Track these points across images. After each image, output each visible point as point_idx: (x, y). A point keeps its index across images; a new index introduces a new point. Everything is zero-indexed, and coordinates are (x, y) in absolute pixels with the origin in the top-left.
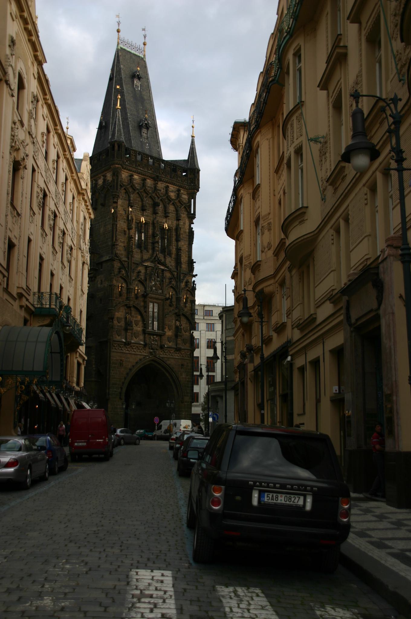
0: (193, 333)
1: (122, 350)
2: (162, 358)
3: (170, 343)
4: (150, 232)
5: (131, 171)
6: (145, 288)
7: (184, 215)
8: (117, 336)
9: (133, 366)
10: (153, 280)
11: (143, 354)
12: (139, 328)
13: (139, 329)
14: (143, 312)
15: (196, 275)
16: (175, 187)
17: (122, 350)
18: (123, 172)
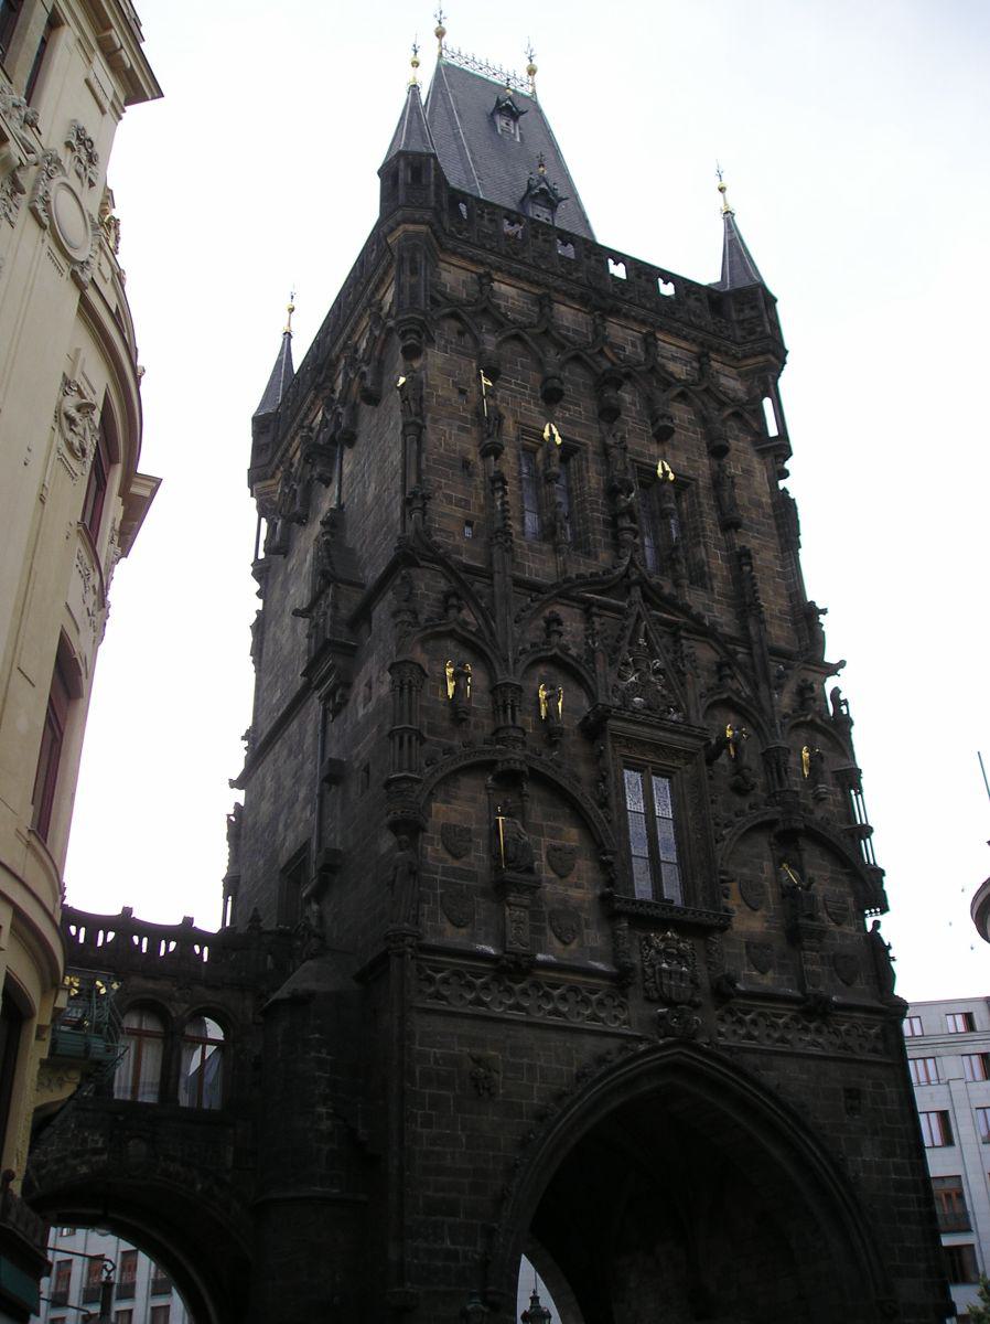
0: (877, 924)
1: (483, 1004)
2: (729, 1049)
3: (763, 973)
4: (593, 482)
5: (481, 263)
6: (591, 695)
7: (740, 444)
8: (448, 925)
9: (559, 1097)
10: (626, 664)
11: (614, 1027)
12: (580, 890)
13: (575, 893)
14: (590, 804)
15: (842, 664)
16: (683, 344)
17: (479, 1002)
18: (443, 265)
